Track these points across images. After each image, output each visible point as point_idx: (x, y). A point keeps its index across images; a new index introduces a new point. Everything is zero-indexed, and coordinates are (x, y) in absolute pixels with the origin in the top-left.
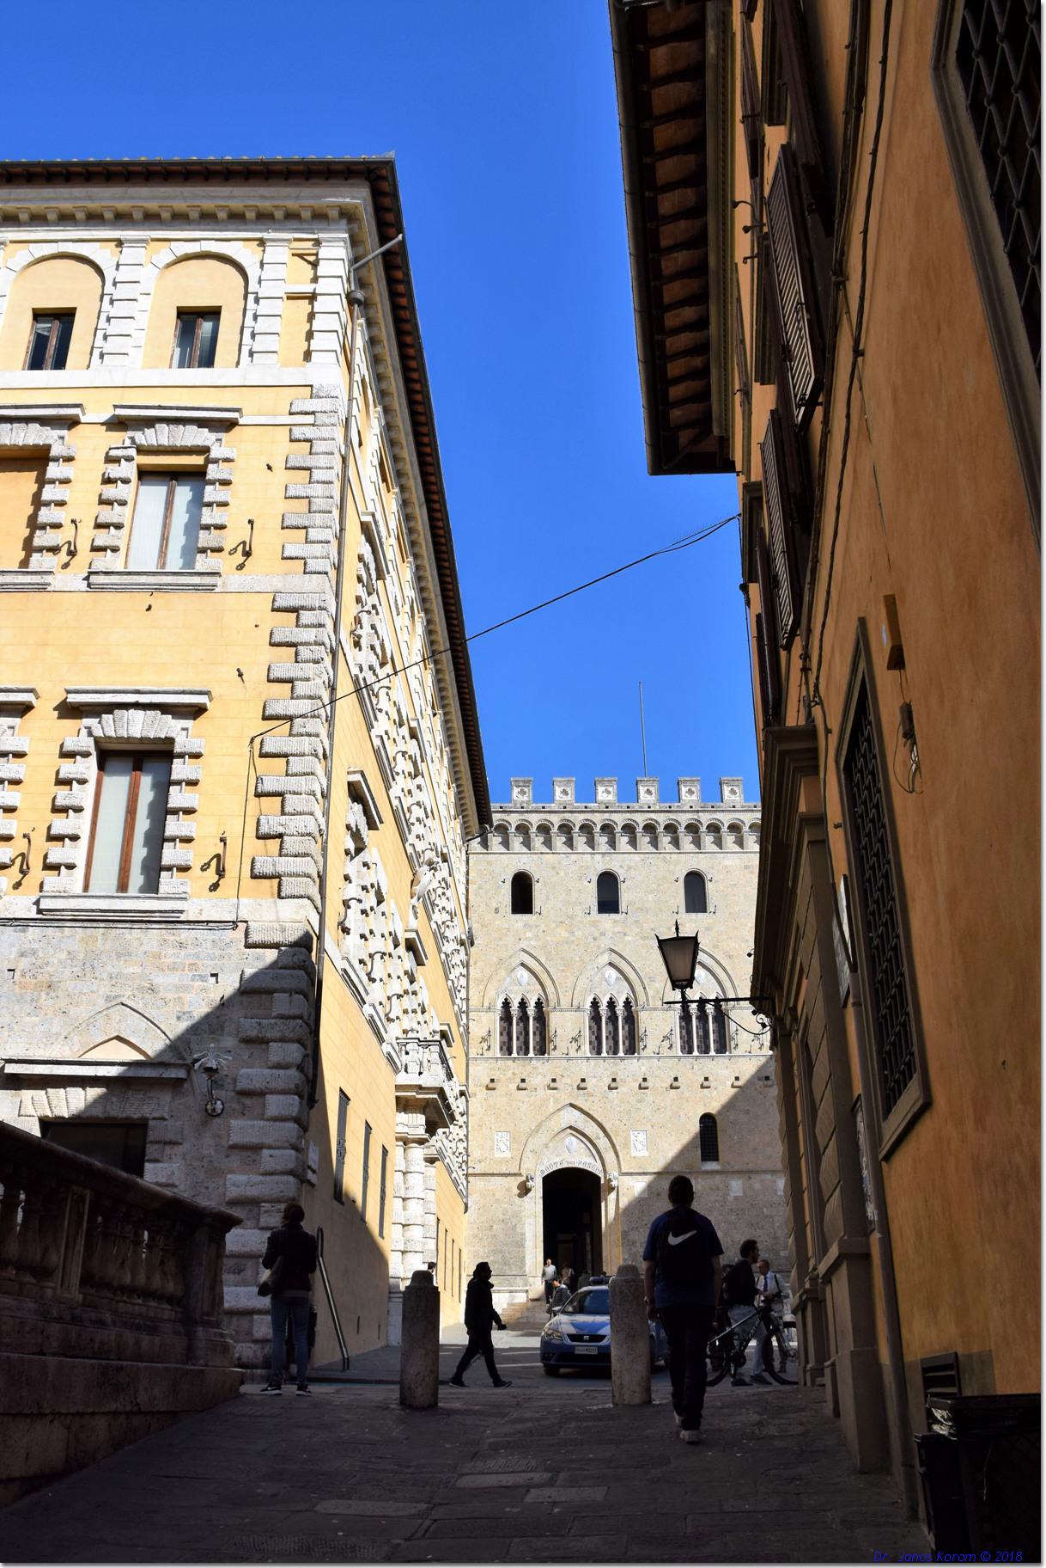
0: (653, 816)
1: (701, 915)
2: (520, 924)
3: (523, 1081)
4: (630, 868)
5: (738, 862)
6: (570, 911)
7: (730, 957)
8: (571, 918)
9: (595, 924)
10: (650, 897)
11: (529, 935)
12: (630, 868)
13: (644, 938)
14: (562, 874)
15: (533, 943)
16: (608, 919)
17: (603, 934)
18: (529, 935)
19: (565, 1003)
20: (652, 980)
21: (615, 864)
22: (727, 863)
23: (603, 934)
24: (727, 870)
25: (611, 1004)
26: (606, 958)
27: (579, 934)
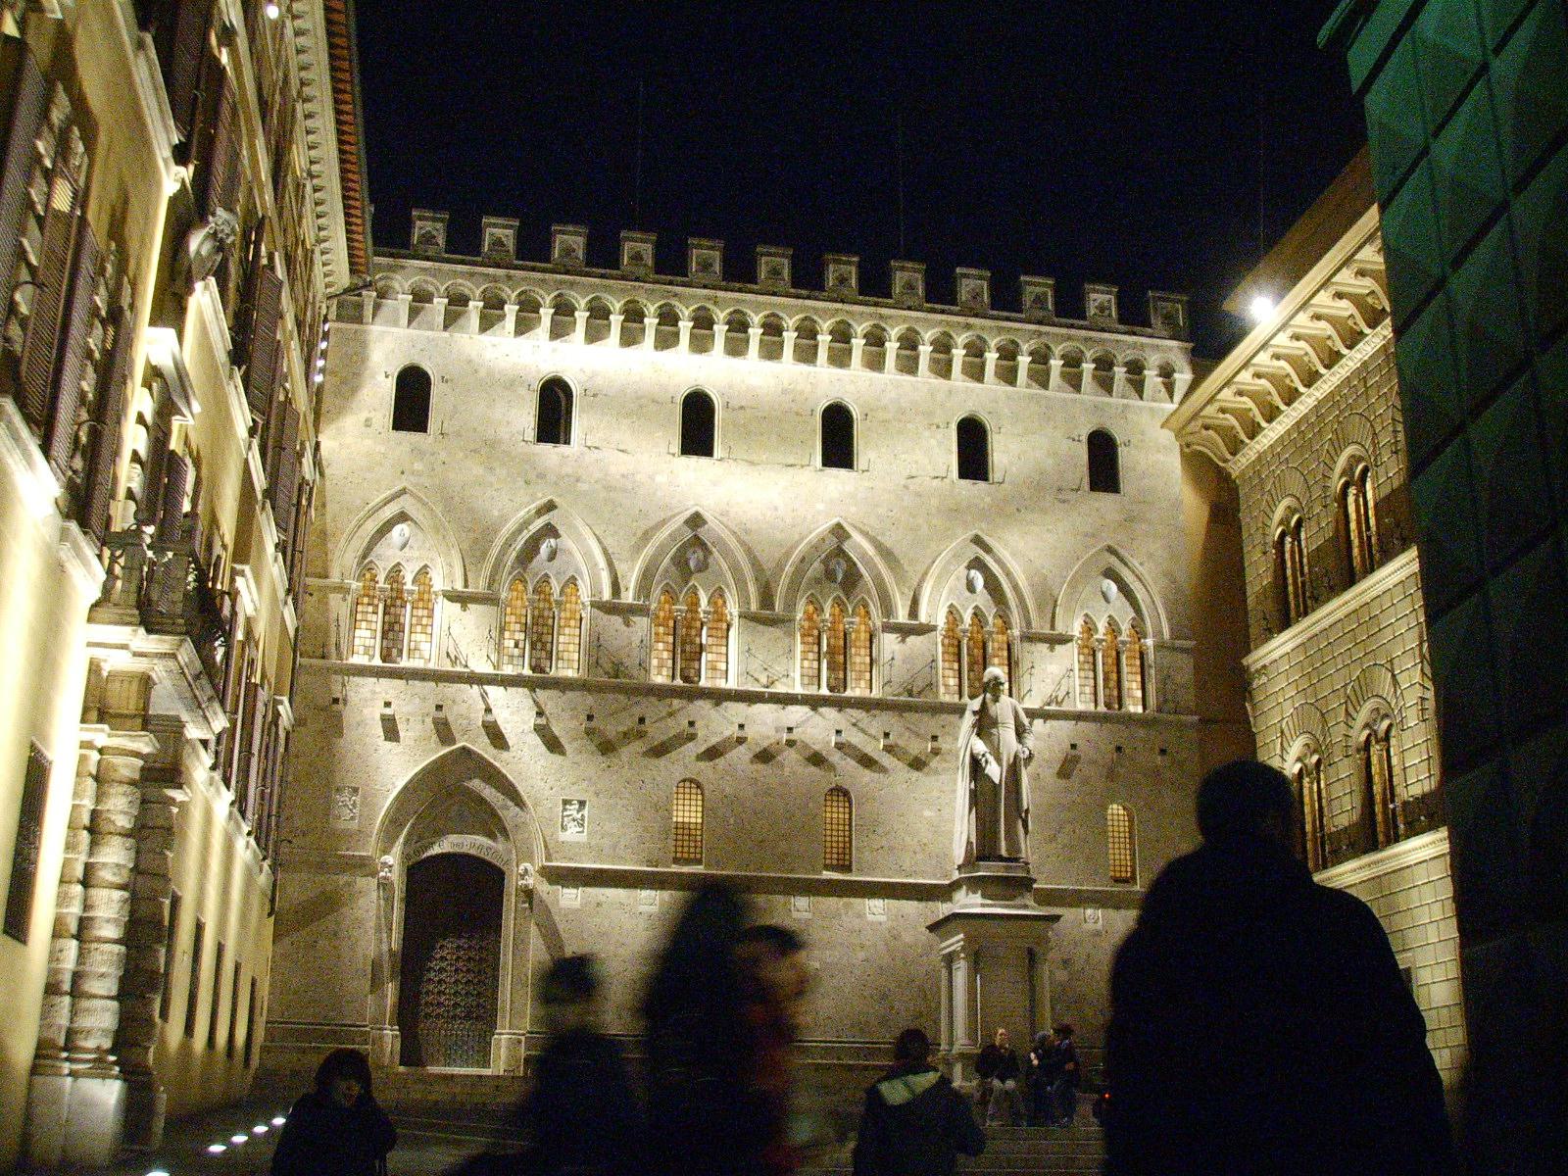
2: (406, 448)
3: (388, 704)
11: (418, 466)
18: (418, 466)
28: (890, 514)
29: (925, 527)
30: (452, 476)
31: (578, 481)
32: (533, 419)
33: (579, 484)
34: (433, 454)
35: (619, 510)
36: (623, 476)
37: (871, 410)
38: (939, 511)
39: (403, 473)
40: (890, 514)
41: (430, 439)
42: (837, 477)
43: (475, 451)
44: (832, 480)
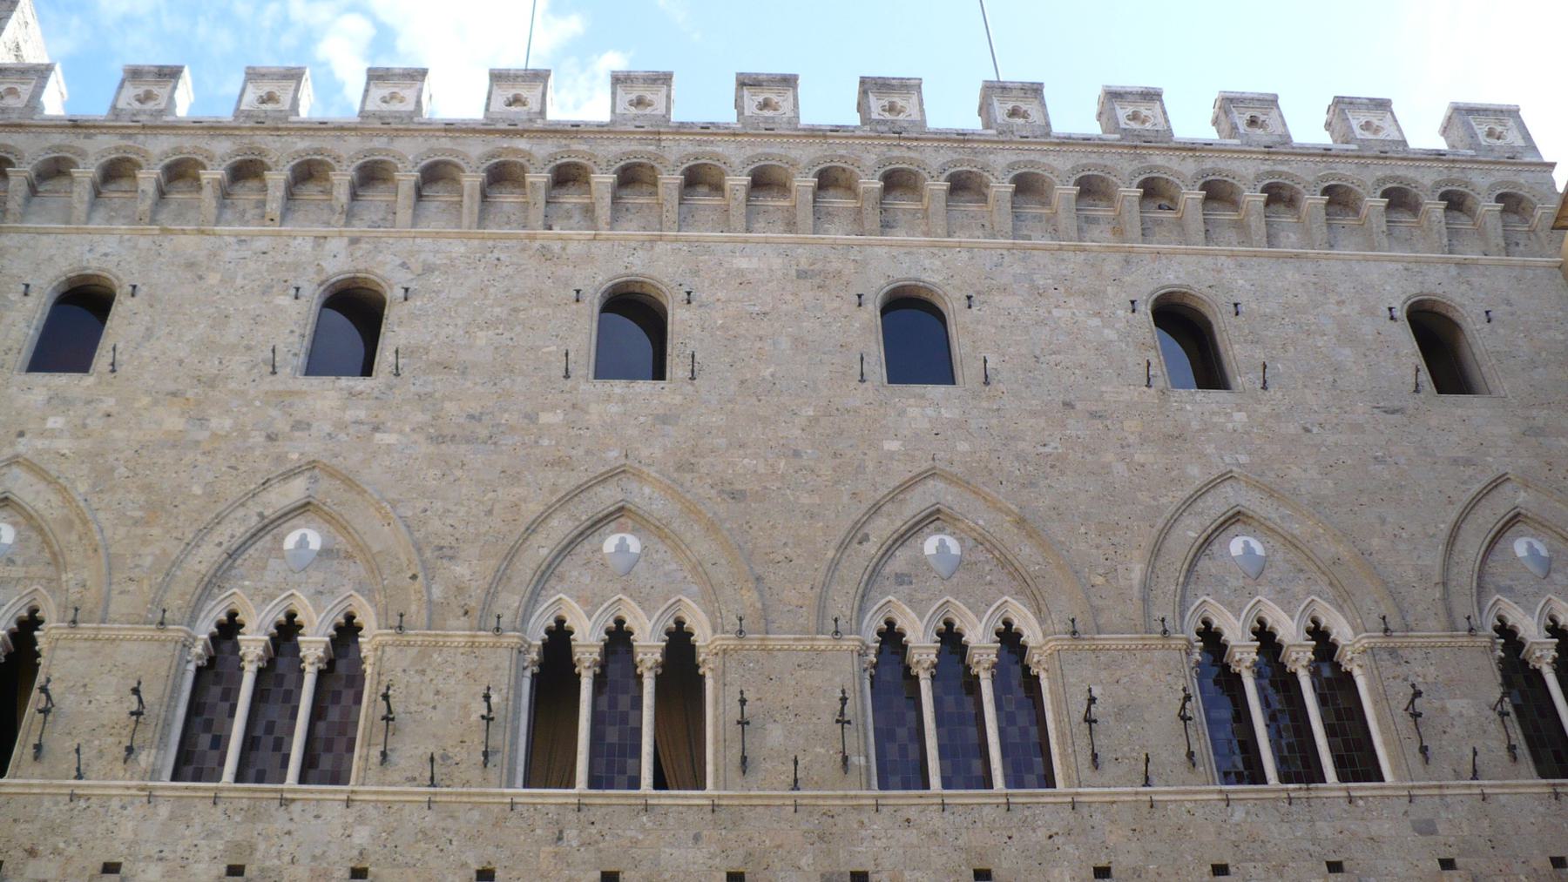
0: (522, 144)
1: (645, 387)
4: (429, 269)
5: (777, 262)
6: (210, 367)
7: (736, 496)
8: (212, 383)
9: (281, 399)
10: (482, 338)
11: (55, 422)
12: (429, 269)
13: (439, 439)
14: (213, 279)
15: (64, 445)
16: (329, 396)
17: (300, 425)
19: (119, 605)
20: (447, 553)
21: (385, 266)
22: (742, 263)
23: (300, 425)
24: (743, 280)
25: (287, 631)
26: (296, 490)
27: (221, 423)
28: (1047, 450)
29: (1120, 468)
30: (118, 434)
31: (376, 429)
32: (295, 338)
33: (378, 436)
34: (88, 402)
35: (458, 473)
36: (471, 417)
37: (979, 293)
38: (1144, 440)
39: (21, 434)
40: (1042, 450)
41: (88, 380)
42: (923, 397)
43: (174, 394)
44: (912, 401)
